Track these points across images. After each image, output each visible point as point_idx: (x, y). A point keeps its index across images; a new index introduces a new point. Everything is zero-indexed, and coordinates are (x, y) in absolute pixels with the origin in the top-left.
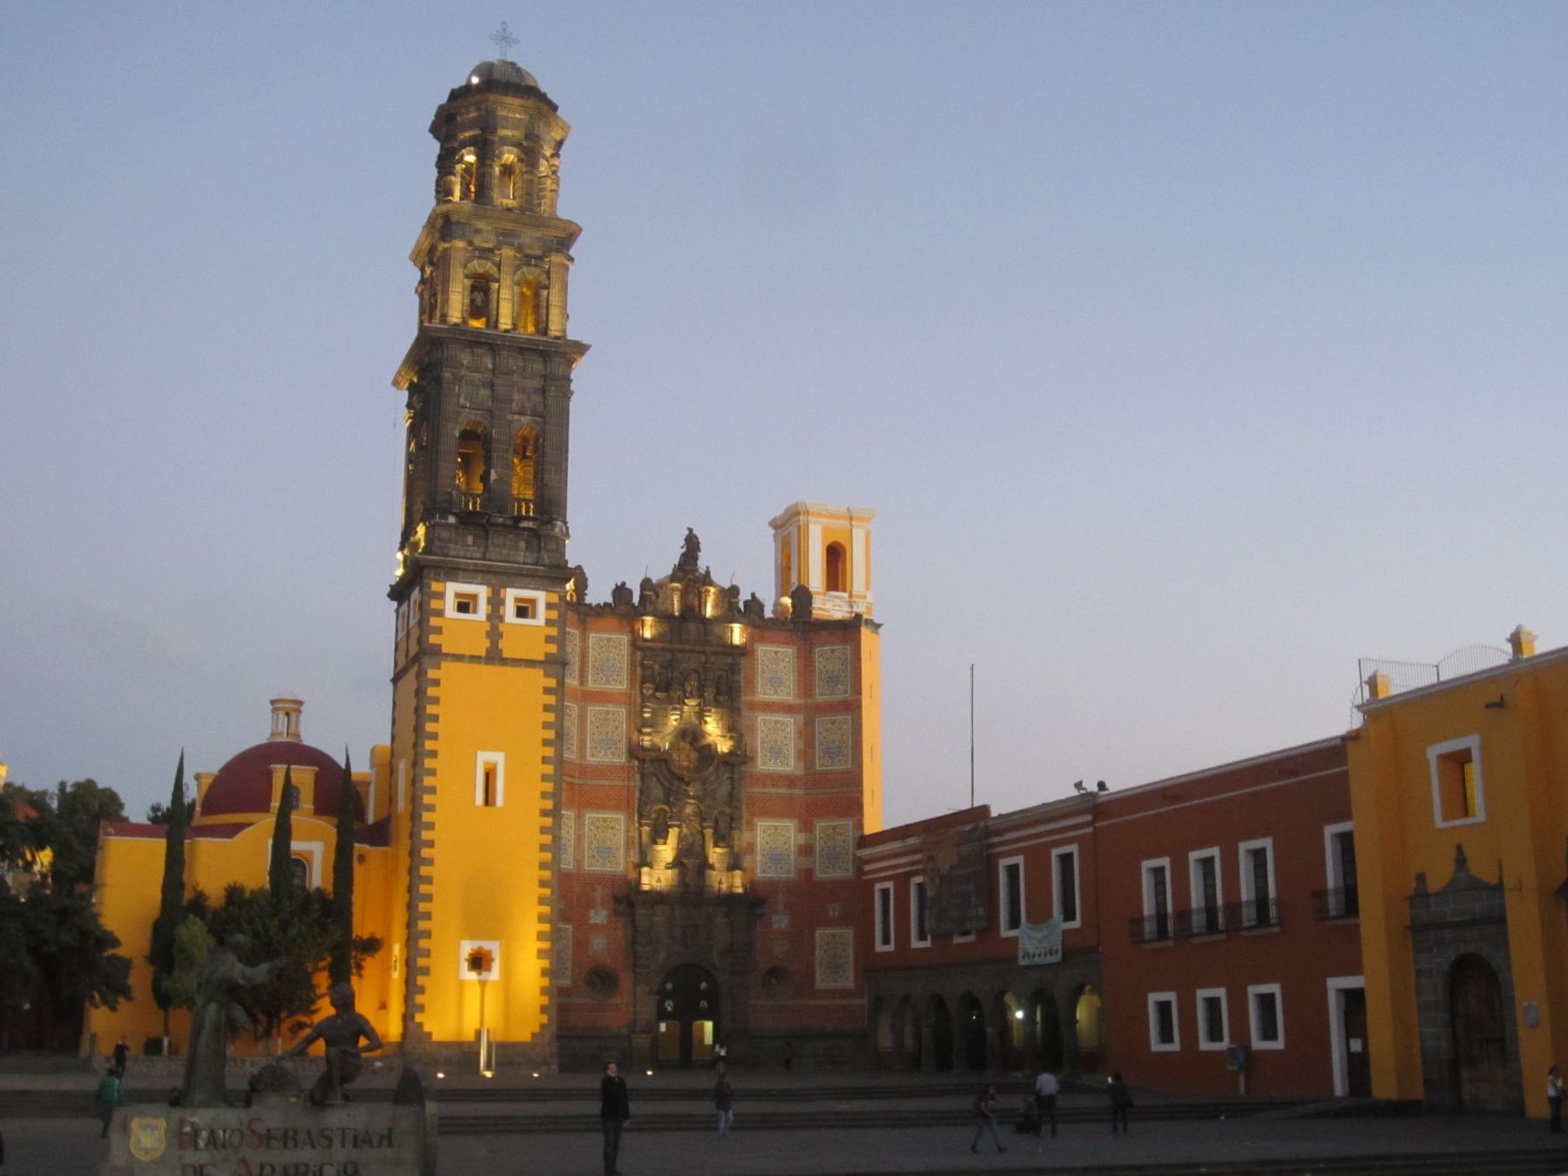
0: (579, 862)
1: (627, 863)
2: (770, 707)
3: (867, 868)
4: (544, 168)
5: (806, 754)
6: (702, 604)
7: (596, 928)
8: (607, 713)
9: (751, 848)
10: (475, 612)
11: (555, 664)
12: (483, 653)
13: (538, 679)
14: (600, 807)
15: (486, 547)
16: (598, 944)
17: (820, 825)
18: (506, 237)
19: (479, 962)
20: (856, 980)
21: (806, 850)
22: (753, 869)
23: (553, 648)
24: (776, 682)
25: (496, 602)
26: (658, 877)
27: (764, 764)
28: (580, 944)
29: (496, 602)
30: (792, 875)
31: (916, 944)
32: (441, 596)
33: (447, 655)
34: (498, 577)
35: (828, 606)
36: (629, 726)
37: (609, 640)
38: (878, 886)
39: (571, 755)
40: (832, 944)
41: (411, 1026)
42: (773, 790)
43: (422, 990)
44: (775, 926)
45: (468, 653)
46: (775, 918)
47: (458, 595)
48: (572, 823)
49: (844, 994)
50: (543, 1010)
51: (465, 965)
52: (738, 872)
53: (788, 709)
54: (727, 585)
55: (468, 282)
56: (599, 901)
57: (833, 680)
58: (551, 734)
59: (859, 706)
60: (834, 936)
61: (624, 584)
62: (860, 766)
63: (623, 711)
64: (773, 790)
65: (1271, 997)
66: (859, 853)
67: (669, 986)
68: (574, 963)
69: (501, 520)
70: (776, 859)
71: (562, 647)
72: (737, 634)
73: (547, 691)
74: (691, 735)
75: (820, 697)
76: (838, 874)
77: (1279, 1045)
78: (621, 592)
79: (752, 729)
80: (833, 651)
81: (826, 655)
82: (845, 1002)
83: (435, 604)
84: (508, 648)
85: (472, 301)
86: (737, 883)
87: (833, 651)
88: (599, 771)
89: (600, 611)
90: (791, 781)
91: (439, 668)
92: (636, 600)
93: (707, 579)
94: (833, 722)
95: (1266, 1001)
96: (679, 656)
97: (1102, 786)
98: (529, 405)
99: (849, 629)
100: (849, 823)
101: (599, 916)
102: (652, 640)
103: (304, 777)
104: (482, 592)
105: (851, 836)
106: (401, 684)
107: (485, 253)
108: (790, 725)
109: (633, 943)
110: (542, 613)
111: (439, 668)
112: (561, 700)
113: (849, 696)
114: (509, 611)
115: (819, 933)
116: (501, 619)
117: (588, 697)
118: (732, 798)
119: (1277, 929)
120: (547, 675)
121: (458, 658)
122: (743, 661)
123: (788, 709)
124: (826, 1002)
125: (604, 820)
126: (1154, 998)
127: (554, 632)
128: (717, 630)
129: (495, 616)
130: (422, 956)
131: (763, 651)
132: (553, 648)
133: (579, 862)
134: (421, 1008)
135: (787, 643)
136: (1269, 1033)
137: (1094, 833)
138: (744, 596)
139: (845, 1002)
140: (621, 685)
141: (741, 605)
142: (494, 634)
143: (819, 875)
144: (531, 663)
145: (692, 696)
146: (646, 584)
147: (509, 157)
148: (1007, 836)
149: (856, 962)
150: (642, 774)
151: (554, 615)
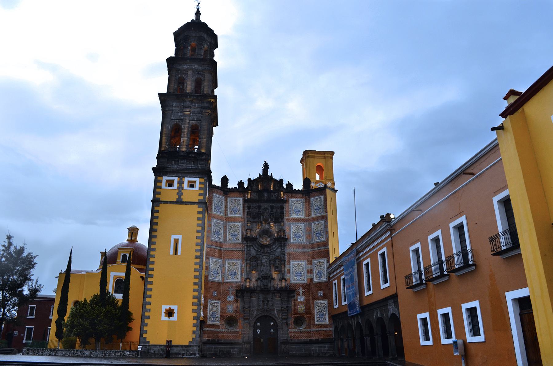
0: (223, 278)
1: (241, 278)
2: (296, 220)
7: (229, 302)
9: (289, 272)
13: (195, 209)
14: (231, 258)
16: (231, 309)
17: (315, 262)
19: (170, 313)
20: (329, 321)
21: (310, 272)
22: (290, 279)
23: (202, 198)
24: (297, 211)
25: (181, 183)
27: (293, 240)
28: (223, 309)
29: (181, 183)
31: (344, 303)
32: (161, 181)
33: (162, 201)
34: (182, 173)
37: (235, 200)
43: (146, 325)
49: (325, 326)
50: (194, 333)
51: (163, 314)
53: (302, 221)
57: (318, 209)
58: (200, 228)
60: (321, 303)
62: (328, 239)
63: (240, 224)
65: (475, 308)
70: (299, 275)
71: (205, 198)
73: (199, 213)
77: (481, 338)
78: (241, 184)
79: (289, 227)
80: (317, 199)
81: (315, 201)
83: (158, 184)
84: (185, 198)
88: (231, 245)
90: (304, 246)
92: (246, 185)
95: (472, 312)
99: (322, 191)
100: (325, 260)
101: (231, 298)
104: (176, 179)
109: (244, 307)
113: (324, 214)
114: (186, 186)
115: (316, 303)
118: (283, 253)
119: (474, 267)
122: (285, 205)
123: (302, 221)
124: (319, 329)
125: (233, 263)
126: (420, 316)
127: (202, 192)
129: (180, 187)
132: (202, 198)
133: (223, 278)
134: (146, 332)
136: (475, 332)
137: (392, 240)
140: (240, 215)
142: (180, 194)
143: (315, 281)
146: (249, 180)
147: (193, 44)
148: (365, 251)
150: (247, 246)
151: (202, 186)
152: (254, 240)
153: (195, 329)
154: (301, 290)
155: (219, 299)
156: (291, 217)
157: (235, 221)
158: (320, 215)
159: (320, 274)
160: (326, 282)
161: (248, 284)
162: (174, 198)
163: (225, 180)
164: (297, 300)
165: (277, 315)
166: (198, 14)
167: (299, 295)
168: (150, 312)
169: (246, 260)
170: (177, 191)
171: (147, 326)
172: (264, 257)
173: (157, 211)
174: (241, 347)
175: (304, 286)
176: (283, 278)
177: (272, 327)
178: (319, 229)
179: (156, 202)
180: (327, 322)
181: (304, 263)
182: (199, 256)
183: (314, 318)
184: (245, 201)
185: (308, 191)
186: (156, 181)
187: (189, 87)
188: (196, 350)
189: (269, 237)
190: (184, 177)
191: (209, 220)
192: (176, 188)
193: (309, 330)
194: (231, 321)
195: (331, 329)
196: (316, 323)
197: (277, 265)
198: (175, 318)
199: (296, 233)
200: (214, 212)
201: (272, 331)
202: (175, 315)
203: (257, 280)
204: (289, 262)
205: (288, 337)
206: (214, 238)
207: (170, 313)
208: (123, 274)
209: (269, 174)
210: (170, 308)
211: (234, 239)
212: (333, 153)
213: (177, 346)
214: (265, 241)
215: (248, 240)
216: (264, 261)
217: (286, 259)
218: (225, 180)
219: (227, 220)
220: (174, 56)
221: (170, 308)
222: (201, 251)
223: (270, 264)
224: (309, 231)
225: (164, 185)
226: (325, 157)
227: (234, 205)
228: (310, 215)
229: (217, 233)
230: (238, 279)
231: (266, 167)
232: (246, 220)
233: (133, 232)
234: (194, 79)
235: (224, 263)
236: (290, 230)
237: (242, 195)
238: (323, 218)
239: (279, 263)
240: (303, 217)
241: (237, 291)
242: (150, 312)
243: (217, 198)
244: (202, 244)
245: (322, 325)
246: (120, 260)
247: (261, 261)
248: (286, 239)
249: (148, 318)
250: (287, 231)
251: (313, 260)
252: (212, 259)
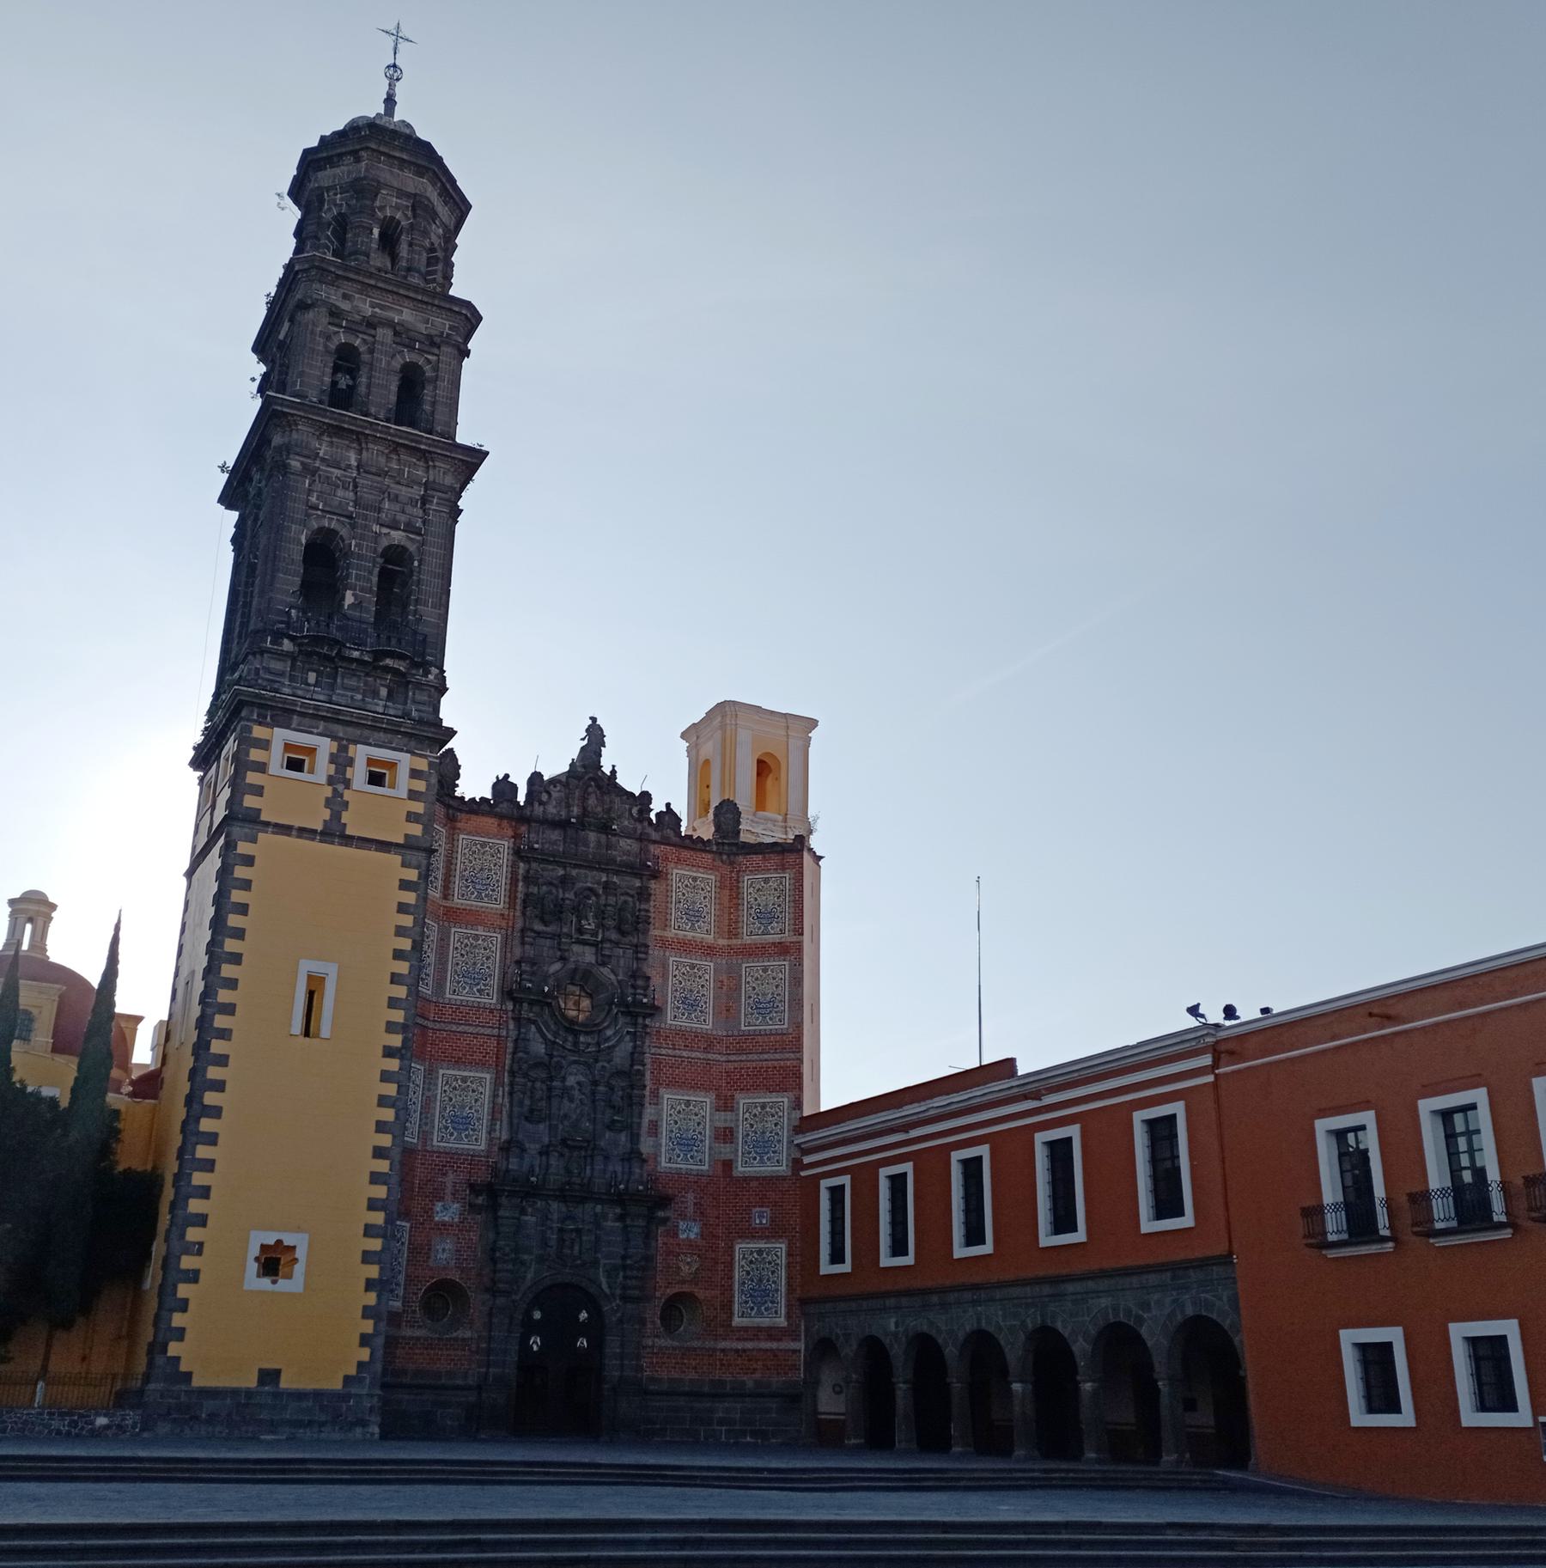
2: (686, 947)
3: (807, 1160)
5: (727, 1010)
8: (476, 937)
9: (654, 1128)
10: (311, 771)
12: (319, 828)
14: (458, 1063)
15: (332, 687)
17: (743, 1101)
20: (788, 1317)
21: (726, 1135)
22: (656, 1156)
23: (416, 830)
24: (694, 916)
25: (341, 761)
27: (673, 1018)
28: (419, 1251)
29: (341, 761)
30: (706, 1168)
32: (265, 745)
35: (758, 830)
36: (504, 958)
37: (484, 845)
38: (825, 1183)
39: (426, 990)
40: (759, 1260)
41: (160, 1360)
42: (684, 1054)
44: (683, 1236)
45: (297, 824)
46: (682, 1225)
47: (288, 747)
48: (419, 1080)
49: (772, 1333)
51: (253, 1267)
53: (709, 951)
56: (449, 1190)
57: (765, 917)
58: (406, 944)
59: (800, 950)
60: (760, 1252)
61: (507, 776)
62: (799, 1026)
64: (684, 1054)
66: (799, 1140)
68: (409, 1279)
69: (356, 654)
70: (686, 1144)
71: (427, 829)
73: (405, 885)
76: (768, 1169)
78: (504, 787)
80: (766, 881)
82: (774, 1345)
83: (255, 755)
85: (334, 383)
87: (766, 881)
89: (476, 807)
90: (709, 1042)
91: (254, 841)
92: (521, 798)
94: (765, 971)
96: (574, 872)
97: (1230, 1012)
98: (402, 518)
100: (785, 1100)
101: (447, 1212)
104: (325, 747)
105: (787, 1120)
106: (195, 877)
109: (493, 1250)
110: (404, 782)
111: (254, 841)
112: (420, 923)
113: (788, 937)
114: (358, 774)
115: (740, 1247)
116: (347, 784)
117: (452, 916)
120: (404, 865)
123: (709, 951)
124: (749, 1345)
125: (464, 1080)
129: (339, 779)
130: (187, 1252)
132: (416, 830)
133: (425, 1136)
135: (713, 869)
137: (1215, 1085)
138: (657, 806)
139: (774, 1345)
142: (336, 804)
143: (740, 1169)
144: (384, 846)
146: (535, 778)
148: (1049, 1100)
149: (791, 1289)
150: (517, 1020)
151: (420, 786)
152: (544, 1002)
153: (368, 1326)
154: (690, 1196)
156: (671, 933)
157: (473, 925)
158: (777, 938)
159: (763, 1146)
160: (784, 1178)
161: (514, 1164)
164: (676, 1235)
165: (604, 1286)
167: (683, 1217)
168: (200, 1253)
169: (512, 1073)
170: (328, 791)
171: (184, 1309)
172: (573, 1069)
174: (472, 1399)
175: (695, 1182)
176: (634, 1156)
177: (584, 1329)
178: (770, 989)
180: (782, 1321)
181: (707, 1100)
182: (398, 1050)
183: (731, 1302)
184: (517, 853)
185: (727, 843)
188: (371, 1409)
189: (590, 996)
190: (356, 742)
192: (323, 780)
193: (709, 1344)
195: (793, 1345)
196: (737, 1321)
197: (617, 1098)
199: (686, 992)
201: (583, 1342)
202: (299, 1269)
203: (545, 1152)
204: (656, 1094)
205: (640, 1369)
207: (273, 1262)
209: (607, 770)
210: (279, 1242)
211: (471, 992)
212: (813, 723)
213: (300, 1395)
214: (578, 1007)
215: (524, 995)
216: (571, 1081)
217: (648, 1083)
220: (451, 292)
221: (279, 1242)
223: (593, 1093)
224: (729, 991)
227: (478, 864)
228: (733, 933)
230: (478, 1142)
232: (519, 925)
234: (397, 363)
236: (665, 976)
237: (510, 833)
238: (785, 948)
239: (625, 1096)
240: (710, 938)
241: (472, 1186)
242: (200, 1253)
245: (759, 1329)
247: (564, 1079)
248: (655, 1010)
249: (193, 1277)
250: (656, 981)
251: (737, 1095)
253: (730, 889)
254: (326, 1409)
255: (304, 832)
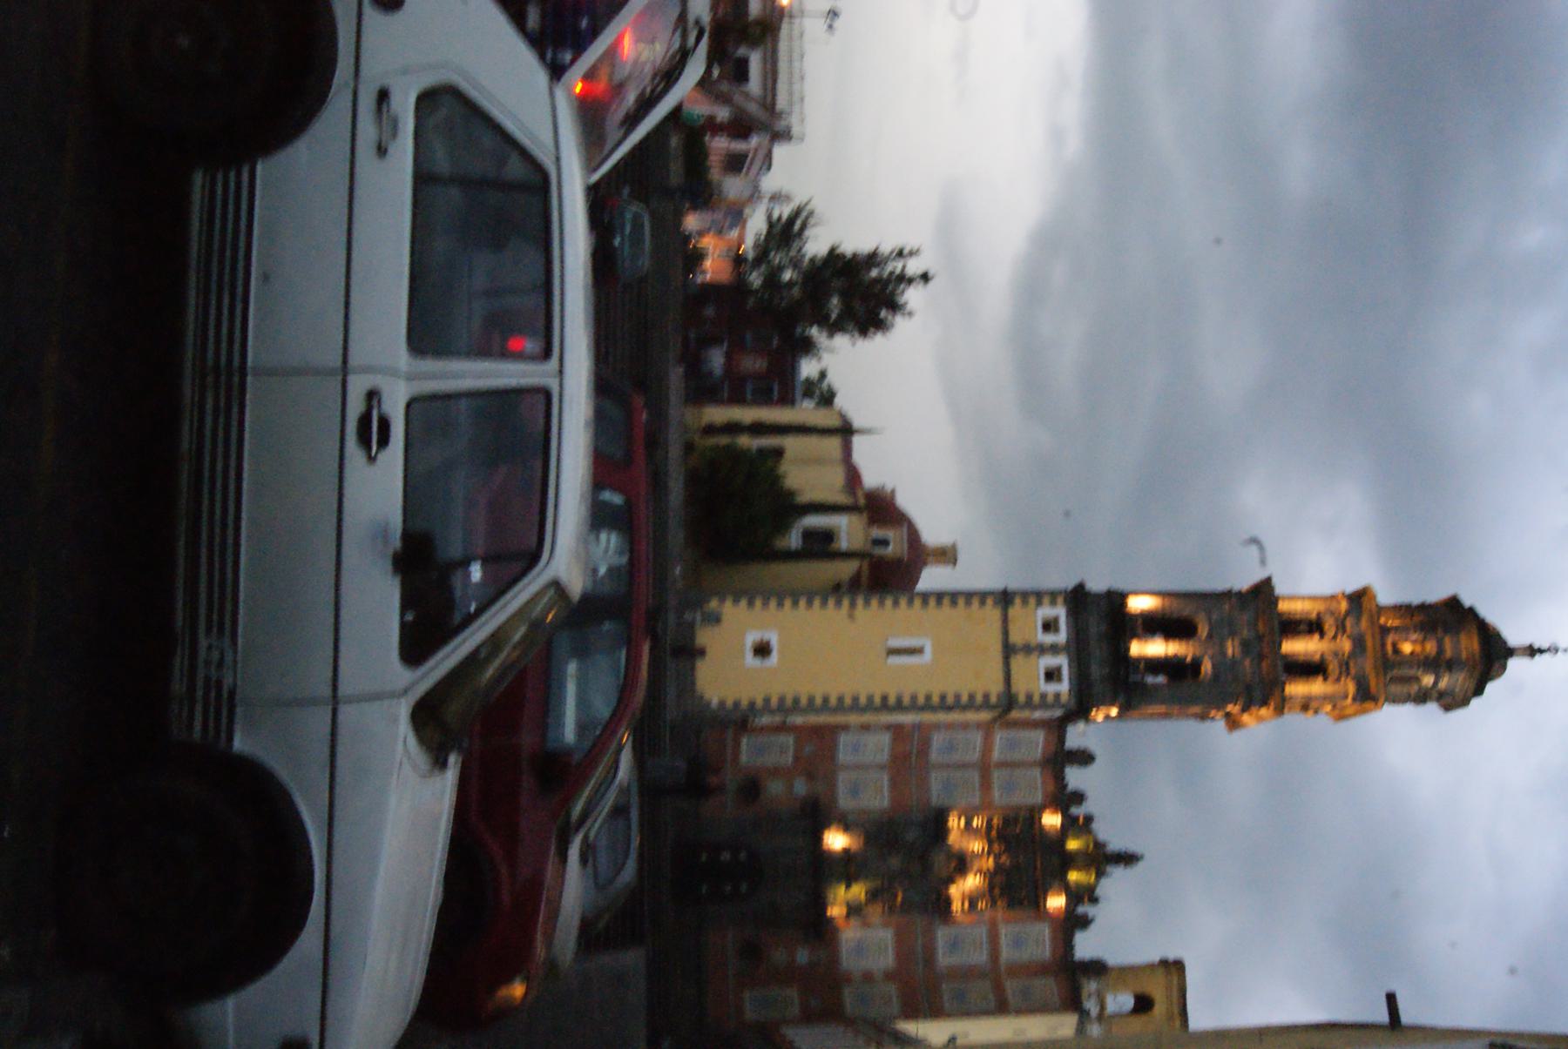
0: (847, 768)
4: (1428, 680)
6: (1079, 869)
7: (791, 786)
11: (1008, 701)
13: (995, 688)
14: (894, 784)
16: (775, 788)
18: (1359, 643)
19: (762, 650)
21: (868, 977)
23: (1022, 698)
24: (1017, 943)
25: (1054, 649)
26: (836, 840)
28: (776, 772)
29: (1054, 649)
32: (1053, 603)
34: (1078, 648)
50: (722, 704)
52: (844, 911)
54: (1099, 892)
55: (1314, 616)
67: (743, 856)
72: (1056, 902)
73: (986, 696)
74: (962, 864)
75: (1010, 986)
78: (1079, 797)
81: (1048, 987)
83: (1046, 600)
84: (1018, 662)
86: (836, 911)
88: (924, 783)
89: (1060, 779)
92: (1074, 810)
93: (1100, 874)
100: (895, 1007)
101: (801, 787)
102: (1041, 827)
103: (896, 546)
104: (1061, 637)
107: (1341, 627)
108: (980, 957)
110: (1051, 688)
114: (1049, 661)
120: (999, 696)
121: (1005, 620)
127: (1036, 699)
128: (1056, 884)
129: (1042, 650)
131: (1044, 931)
141: (1081, 909)
145: (996, 862)
155: (797, 758)
158: (1010, 997)
162: (1016, 638)
163: (1084, 758)
166: (1532, 651)
170: (1033, 644)
173: (983, 603)
175: (834, 959)
179: (1005, 598)
186: (1053, 596)
187: (1298, 647)
191: (979, 726)
194: (751, 788)
198: (750, 660)
200: (999, 737)
206: (938, 740)
207: (762, 650)
208: (843, 544)
209: (1110, 869)
218: (1084, 758)
219: (985, 769)
222: (899, 707)
225: (1046, 612)
226: (1170, 1018)
229: (951, 747)
231: (1127, 859)
233: (947, 555)
234: (1329, 658)
235: (881, 767)
243: (1036, 743)
244: (914, 706)
246: (877, 532)
252: (885, 739)
253: (1041, 969)
254: (687, 683)
255: (1006, 633)
